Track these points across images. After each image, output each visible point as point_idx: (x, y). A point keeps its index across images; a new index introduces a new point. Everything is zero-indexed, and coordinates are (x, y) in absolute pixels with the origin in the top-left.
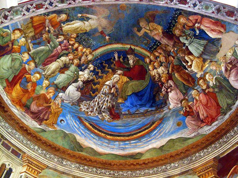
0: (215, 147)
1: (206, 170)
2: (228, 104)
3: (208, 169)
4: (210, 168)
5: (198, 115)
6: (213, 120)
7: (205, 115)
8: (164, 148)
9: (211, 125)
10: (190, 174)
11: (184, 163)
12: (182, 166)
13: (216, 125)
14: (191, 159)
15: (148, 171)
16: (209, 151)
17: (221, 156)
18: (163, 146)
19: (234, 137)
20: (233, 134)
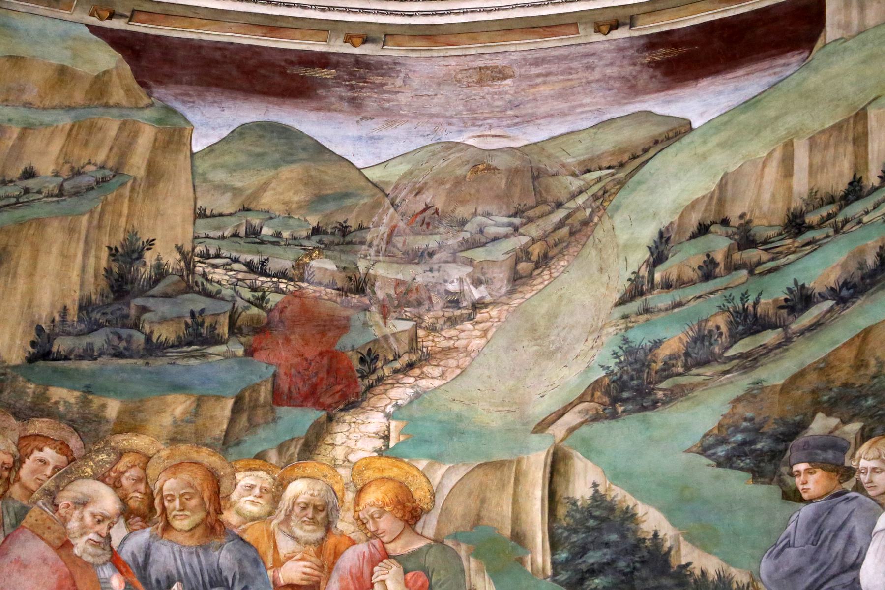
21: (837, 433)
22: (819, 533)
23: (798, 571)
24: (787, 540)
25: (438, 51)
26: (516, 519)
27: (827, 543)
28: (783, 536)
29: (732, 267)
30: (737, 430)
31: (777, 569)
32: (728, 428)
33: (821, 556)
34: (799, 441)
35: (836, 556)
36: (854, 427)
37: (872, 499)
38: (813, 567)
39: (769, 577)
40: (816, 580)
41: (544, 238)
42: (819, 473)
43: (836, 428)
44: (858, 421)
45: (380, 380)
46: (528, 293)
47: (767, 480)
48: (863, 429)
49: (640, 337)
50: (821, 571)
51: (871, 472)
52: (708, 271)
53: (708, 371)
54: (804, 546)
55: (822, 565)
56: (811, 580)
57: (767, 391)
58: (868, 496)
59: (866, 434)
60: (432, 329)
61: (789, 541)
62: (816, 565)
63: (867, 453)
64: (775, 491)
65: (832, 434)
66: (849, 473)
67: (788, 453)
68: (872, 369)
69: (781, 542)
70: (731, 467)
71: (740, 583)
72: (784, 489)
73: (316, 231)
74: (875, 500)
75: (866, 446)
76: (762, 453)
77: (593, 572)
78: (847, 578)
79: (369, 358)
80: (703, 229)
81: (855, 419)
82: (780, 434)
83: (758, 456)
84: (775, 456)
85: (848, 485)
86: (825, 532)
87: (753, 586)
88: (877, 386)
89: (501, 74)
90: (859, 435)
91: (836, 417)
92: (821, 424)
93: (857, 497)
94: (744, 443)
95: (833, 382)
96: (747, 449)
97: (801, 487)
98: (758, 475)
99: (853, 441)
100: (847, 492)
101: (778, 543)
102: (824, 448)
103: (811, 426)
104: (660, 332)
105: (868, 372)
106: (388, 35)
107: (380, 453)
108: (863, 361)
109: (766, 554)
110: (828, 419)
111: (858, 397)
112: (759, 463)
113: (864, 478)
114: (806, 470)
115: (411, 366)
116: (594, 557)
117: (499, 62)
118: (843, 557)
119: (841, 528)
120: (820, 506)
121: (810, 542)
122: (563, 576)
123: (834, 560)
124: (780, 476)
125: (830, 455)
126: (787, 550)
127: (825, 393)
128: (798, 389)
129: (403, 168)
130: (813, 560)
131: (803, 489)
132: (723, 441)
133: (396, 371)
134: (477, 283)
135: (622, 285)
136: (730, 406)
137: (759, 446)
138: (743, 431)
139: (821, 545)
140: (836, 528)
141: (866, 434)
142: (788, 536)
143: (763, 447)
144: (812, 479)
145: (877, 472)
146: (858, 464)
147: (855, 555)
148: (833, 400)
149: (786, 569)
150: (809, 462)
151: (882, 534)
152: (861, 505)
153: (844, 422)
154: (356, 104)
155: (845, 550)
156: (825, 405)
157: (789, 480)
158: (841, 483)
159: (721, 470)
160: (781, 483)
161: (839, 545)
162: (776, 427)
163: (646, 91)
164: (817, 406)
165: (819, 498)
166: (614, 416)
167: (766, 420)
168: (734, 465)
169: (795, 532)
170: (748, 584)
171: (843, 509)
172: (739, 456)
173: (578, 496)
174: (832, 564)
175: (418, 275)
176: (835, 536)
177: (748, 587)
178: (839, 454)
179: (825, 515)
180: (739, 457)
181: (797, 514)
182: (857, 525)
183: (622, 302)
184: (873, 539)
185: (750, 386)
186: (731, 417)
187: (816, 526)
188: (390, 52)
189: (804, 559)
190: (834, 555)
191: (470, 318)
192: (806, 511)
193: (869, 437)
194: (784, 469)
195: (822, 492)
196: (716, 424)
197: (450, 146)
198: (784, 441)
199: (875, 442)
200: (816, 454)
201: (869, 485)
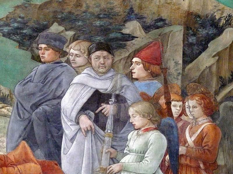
21: (62, 34)
22: (46, 78)
23: (33, 94)
24: (31, 78)
27: (49, 84)
28: (28, 76)
30: (15, 21)
31: (23, 91)
32: (11, 19)
33: (45, 89)
34: (44, 33)
35: (52, 91)
36: (70, 33)
37: (73, 68)
38: (40, 94)
39: (19, 94)
40: (40, 100)
42: (51, 51)
43: (62, 32)
44: (73, 31)
47: (25, 48)
48: (75, 35)
50: (44, 96)
51: (75, 56)
54: (37, 83)
55: (44, 94)
56: (38, 99)
57: (33, 6)
58: (72, 66)
59: (75, 38)
61: (31, 79)
62: (42, 93)
63: (75, 47)
64: (29, 54)
65: (60, 34)
66: (65, 54)
67: (38, 38)
68: (84, 8)
69: (27, 79)
70: (9, 38)
71: (4, 94)
72: (33, 54)
74: (74, 69)
75: (74, 43)
76: (25, 35)
78: (55, 102)
81: (72, 29)
82: (36, 28)
83: (24, 36)
84: (31, 38)
85: (64, 59)
86: (49, 79)
87: (10, 97)
88: (84, 17)
90: (72, 38)
91: (63, 26)
92: (55, 28)
93: (66, 66)
94: (18, 28)
95: (65, 10)
96: (18, 31)
97: (41, 55)
98: (21, 45)
99: (69, 40)
100: (62, 62)
101: (26, 79)
102: (55, 40)
103: (50, 28)
105: (81, 9)
108: (80, 3)
109: (19, 83)
110: (59, 26)
111: (75, 20)
112: (23, 39)
113: (71, 58)
114: (44, 48)
118: (55, 92)
119: (57, 78)
120: (48, 66)
121: (41, 82)
123: (51, 93)
124: (32, 48)
125: (57, 43)
126: (29, 83)
127: (60, 14)
128: (47, 9)
130: (41, 90)
131: (42, 57)
132: (8, 25)
136: (14, 9)
137: (24, 31)
138: (18, 22)
139: (46, 85)
140: (54, 78)
141: (75, 38)
142: (31, 77)
143: (26, 32)
144: (47, 53)
145: (78, 57)
146: (69, 51)
147: (61, 92)
148: (63, 18)
149: (28, 92)
150: (47, 45)
151: (75, 85)
152: (68, 70)
153: (66, 30)
155: (56, 89)
156: (59, 20)
157: (36, 51)
158: (60, 58)
159: (4, 39)
160: (32, 51)
161: (54, 86)
162: (34, 24)
164: (55, 19)
165: (49, 62)
167: (29, 20)
168: (11, 37)
169: (35, 75)
170: (8, 95)
171: (59, 70)
172: (14, 34)
174: (50, 94)
176: (53, 81)
177: (8, 97)
178: (61, 44)
179: (50, 71)
180: (14, 34)
181: (37, 67)
182: (64, 79)
184: (70, 87)
185: (25, 2)
186: (13, 14)
187: (45, 75)
189: (36, 89)
190: (51, 90)
192: (42, 67)
193: (77, 40)
194: (34, 45)
195: (50, 60)
196: (6, 16)
198: (36, 32)
199: (79, 42)
200: (50, 41)
201: (73, 62)
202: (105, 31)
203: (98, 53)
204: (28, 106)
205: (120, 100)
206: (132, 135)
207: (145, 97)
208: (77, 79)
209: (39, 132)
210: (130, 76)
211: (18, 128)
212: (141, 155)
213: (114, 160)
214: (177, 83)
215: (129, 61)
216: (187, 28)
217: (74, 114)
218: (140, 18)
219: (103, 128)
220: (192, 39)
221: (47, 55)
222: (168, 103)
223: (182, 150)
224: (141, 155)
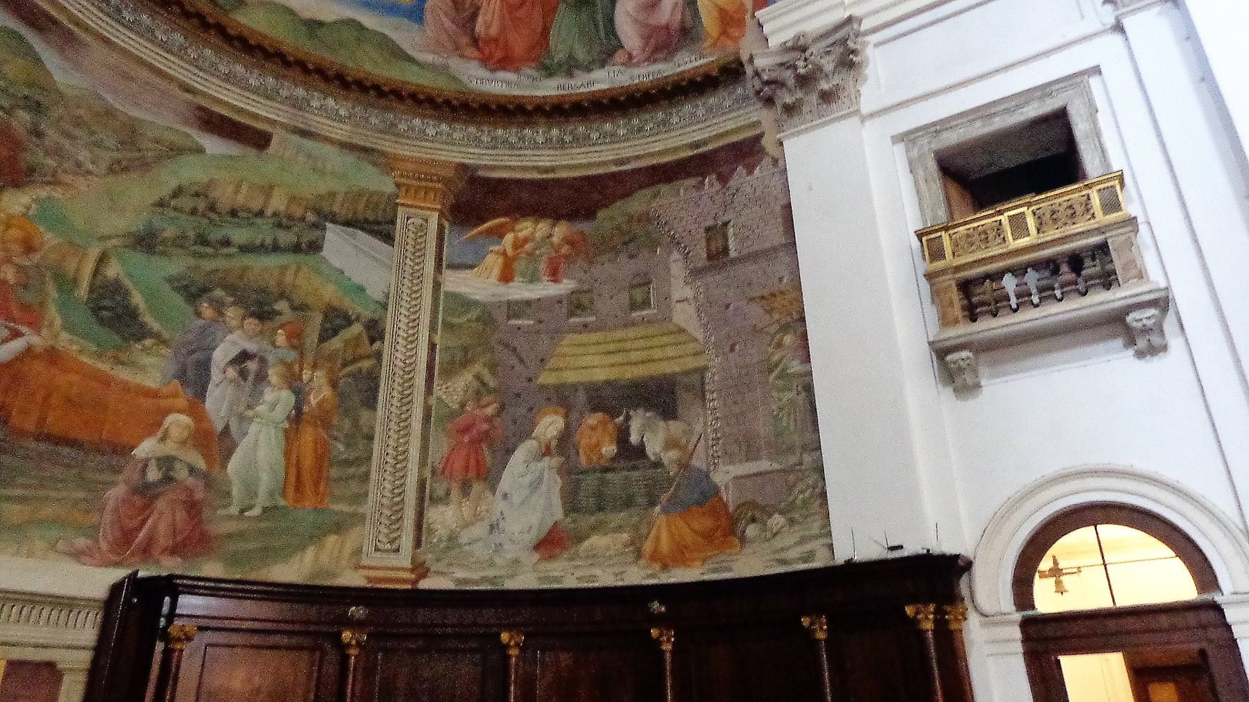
0: (476, 138)
1: (426, 180)
2: (571, 57)
3: (431, 181)
4: (439, 181)
5: (473, 17)
6: (506, 62)
7: (493, 31)
8: (321, 33)
9: (493, 71)
10: (375, 164)
11: (367, 119)
12: (357, 125)
13: (508, 83)
14: (393, 125)
15: (243, 70)
16: (455, 135)
17: (481, 173)
18: (321, 24)
19: (538, 148)
20: (540, 139)
25: (106, 51)
26: (77, 270)
29: (204, 216)
41: (129, 160)
45: (33, 182)
46: (110, 179)
49: (157, 223)
52: (194, 212)
53: (180, 251)
60: (65, 171)
73: (26, 98)
77: (105, 308)
79: (31, 171)
80: (197, 195)
89: (132, 79)
92: (219, 293)
104: (166, 225)
106: (87, 29)
107: (24, 215)
115: (49, 183)
116: (106, 303)
117: (133, 73)
122: (91, 305)
129: (76, 92)
133: (43, 182)
134: (93, 163)
135: (156, 198)
154: (62, 50)
163: (191, 125)
166: (134, 249)
173: (109, 275)
175: (67, 144)
182: (219, 334)
183: (154, 205)
188: (88, 38)
191: (83, 176)
192: (201, 322)
197: (100, 97)
202: (261, 304)
203: (250, 320)
204: (184, 351)
205: (263, 361)
206: (267, 390)
207: (282, 362)
208: (230, 337)
209: (191, 373)
210: (274, 344)
211: (172, 368)
212: (273, 407)
213: (249, 407)
214: (310, 358)
215: (274, 331)
216: (326, 316)
217: (224, 363)
218: (289, 299)
219: (245, 379)
220: (328, 325)
221: (207, 310)
222: (301, 370)
223: (306, 409)
224: (273, 407)
